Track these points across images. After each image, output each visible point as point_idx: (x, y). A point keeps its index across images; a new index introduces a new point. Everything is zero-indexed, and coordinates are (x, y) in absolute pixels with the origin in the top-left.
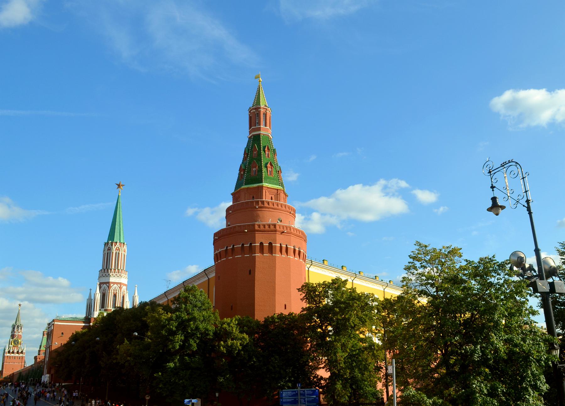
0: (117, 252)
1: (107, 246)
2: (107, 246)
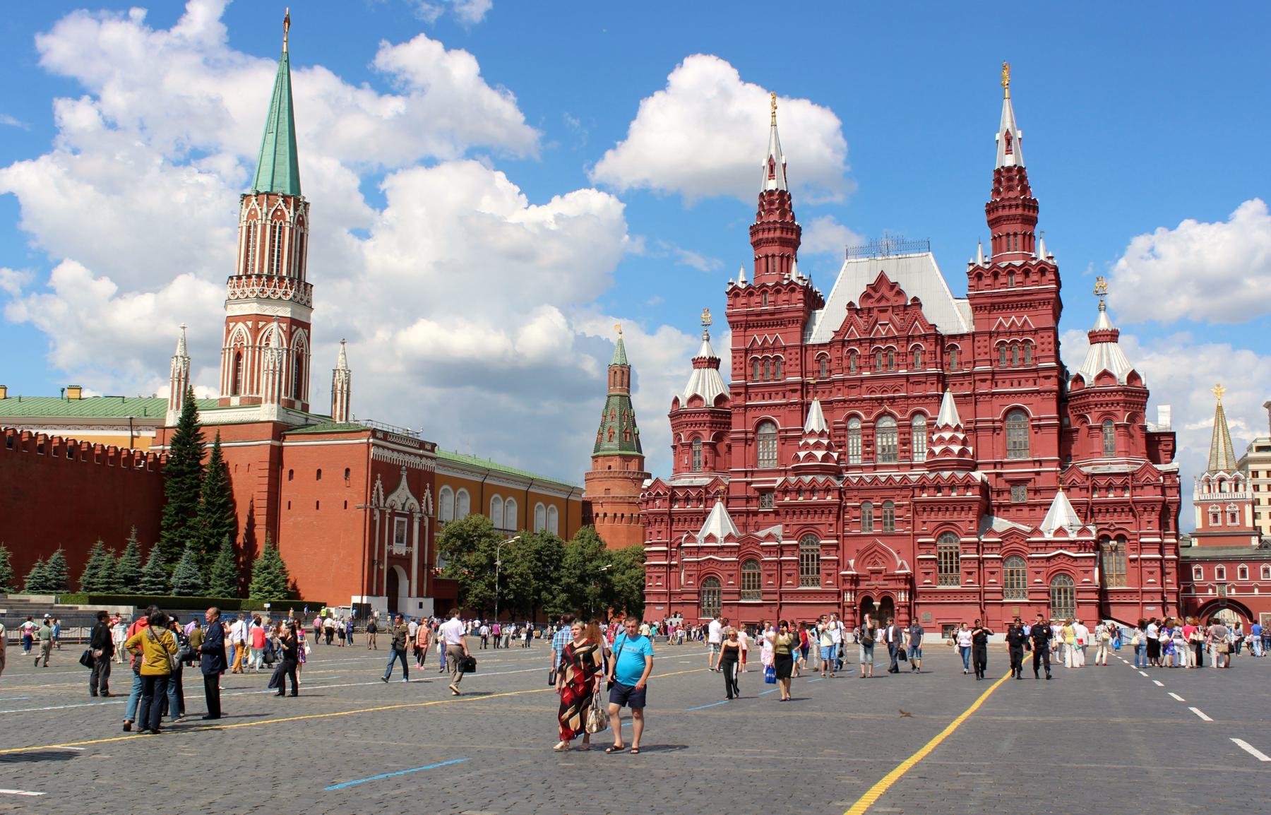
0: (278, 225)
1: (247, 207)
2: (247, 207)
